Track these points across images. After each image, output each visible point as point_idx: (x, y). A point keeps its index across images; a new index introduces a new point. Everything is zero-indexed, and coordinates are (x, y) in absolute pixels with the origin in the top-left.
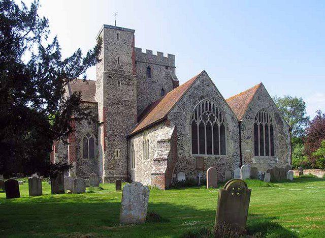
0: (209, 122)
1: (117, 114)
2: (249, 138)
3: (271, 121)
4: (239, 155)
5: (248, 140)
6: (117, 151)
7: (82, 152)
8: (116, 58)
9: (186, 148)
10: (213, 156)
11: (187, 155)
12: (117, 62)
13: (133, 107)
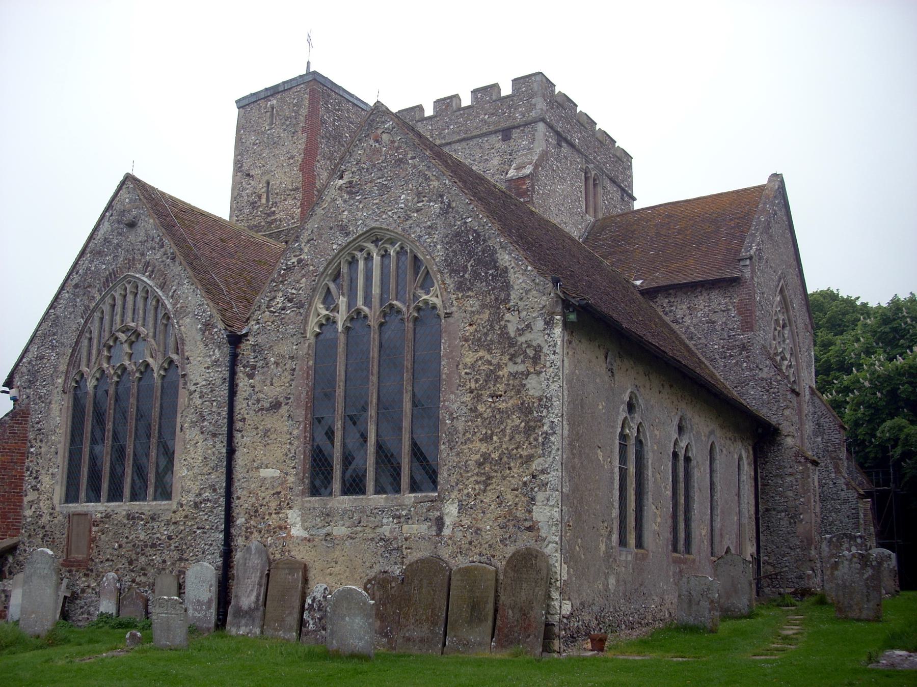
2: (276, 406)
3: (426, 283)
4: (222, 500)
5: (270, 421)
8: (261, 188)
9: (46, 480)
10: (121, 508)
11: (44, 506)
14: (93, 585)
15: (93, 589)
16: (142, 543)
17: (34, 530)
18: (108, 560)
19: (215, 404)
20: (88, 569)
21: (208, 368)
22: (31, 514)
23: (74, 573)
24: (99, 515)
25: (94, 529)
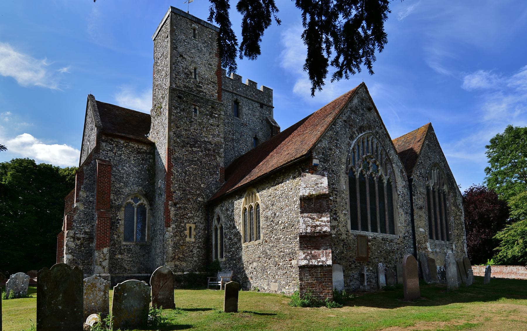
0: (371, 175)
1: (191, 162)
6: (190, 228)
7: (122, 229)
10: (380, 235)
12: (193, 74)
13: (218, 154)
14: (371, 269)
15: (371, 271)
16: (388, 251)
17: (337, 241)
18: (376, 258)
19: (405, 201)
20: (368, 262)
21: (402, 187)
22: (335, 233)
23: (362, 263)
24: (370, 237)
25: (369, 243)
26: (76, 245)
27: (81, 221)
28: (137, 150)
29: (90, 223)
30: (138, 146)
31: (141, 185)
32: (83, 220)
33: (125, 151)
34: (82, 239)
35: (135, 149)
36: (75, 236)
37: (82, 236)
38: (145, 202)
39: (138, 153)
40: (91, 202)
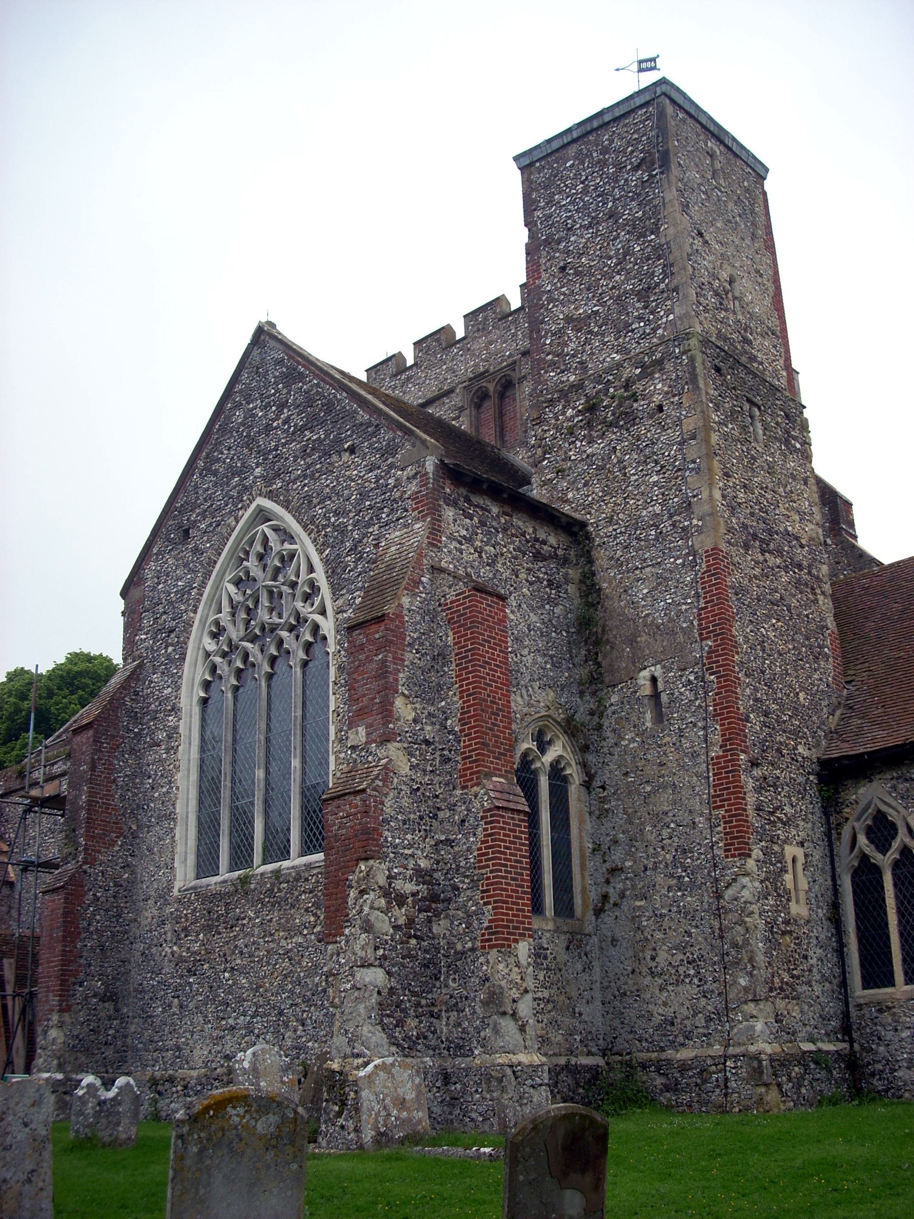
26: (396, 928)
27: (404, 822)
28: (533, 546)
29: (431, 831)
30: (535, 530)
31: (551, 683)
32: (409, 819)
33: (505, 547)
34: (410, 900)
35: (528, 542)
36: (390, 884)
37: (409, 887)
38: (569, 756)
39: (538, 556)
40: (427, 743)
